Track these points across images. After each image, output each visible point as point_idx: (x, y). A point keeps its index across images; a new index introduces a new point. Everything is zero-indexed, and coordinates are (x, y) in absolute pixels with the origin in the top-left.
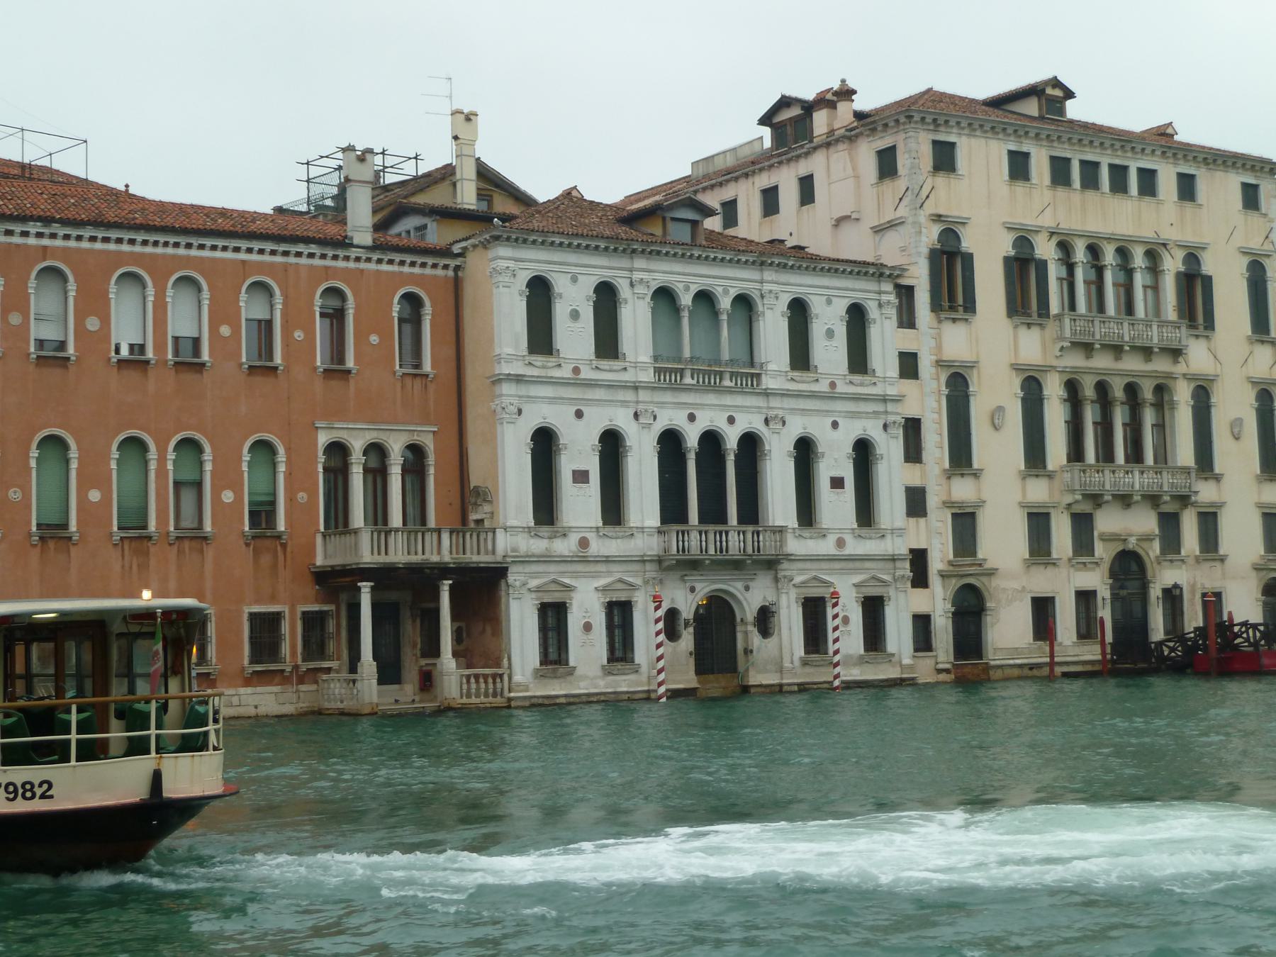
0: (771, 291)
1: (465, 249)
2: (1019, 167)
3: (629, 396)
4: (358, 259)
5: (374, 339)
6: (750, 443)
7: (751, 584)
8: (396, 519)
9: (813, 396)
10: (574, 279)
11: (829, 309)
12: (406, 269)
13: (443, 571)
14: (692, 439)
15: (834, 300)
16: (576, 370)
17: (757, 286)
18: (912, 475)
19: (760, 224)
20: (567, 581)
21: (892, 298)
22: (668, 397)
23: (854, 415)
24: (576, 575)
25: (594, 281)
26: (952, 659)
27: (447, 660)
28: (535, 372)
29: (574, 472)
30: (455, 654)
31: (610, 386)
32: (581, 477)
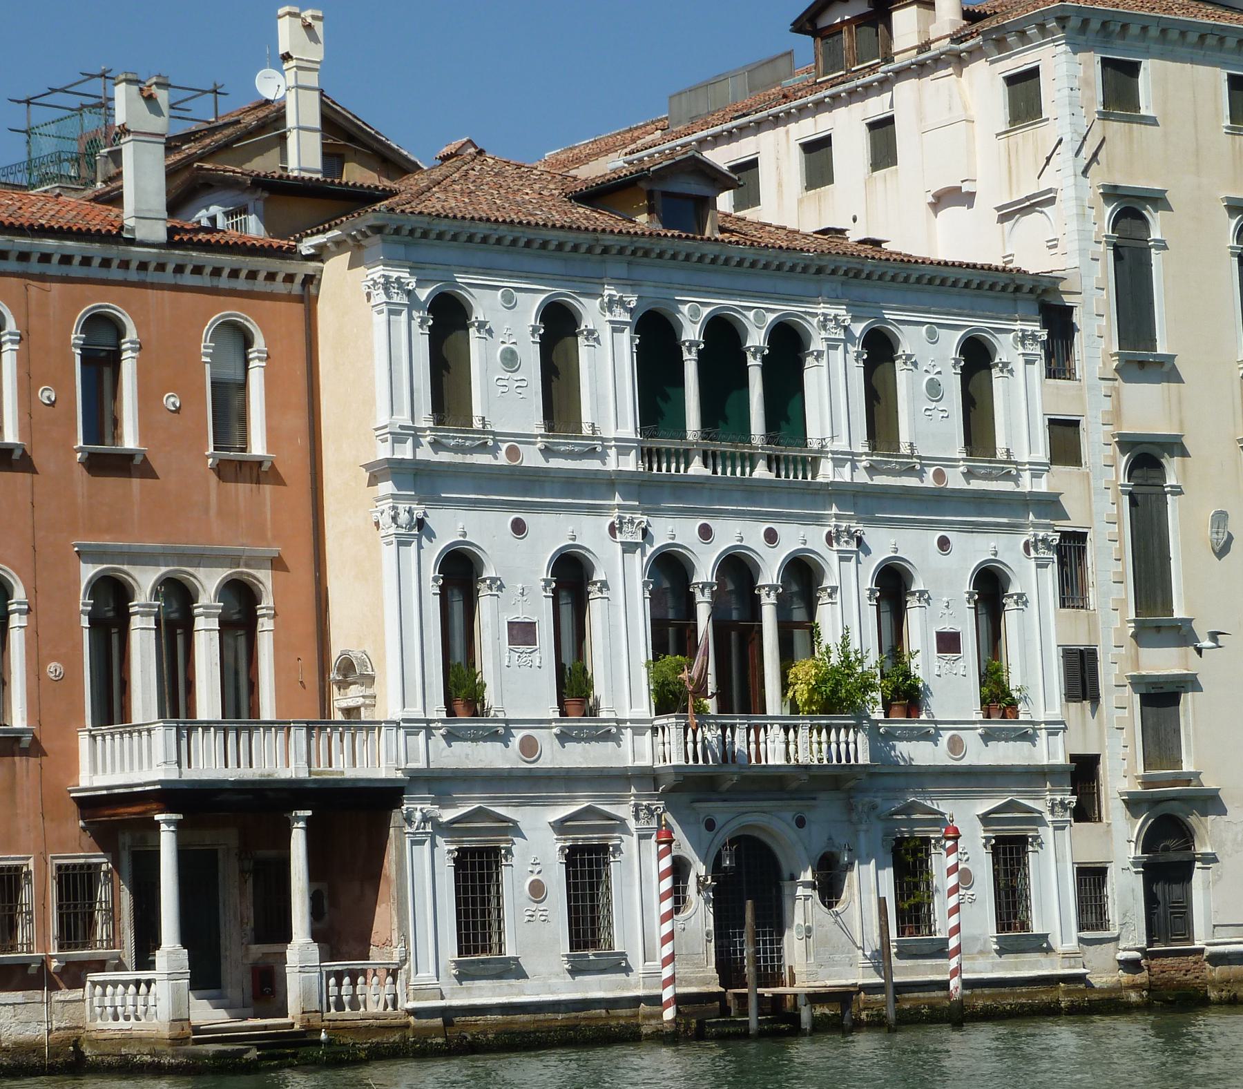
1: (321, 248)
7: (809, 816)
15: (942, 332)
19: (800, 201)
27: (301, 949)
30: (316, 935)
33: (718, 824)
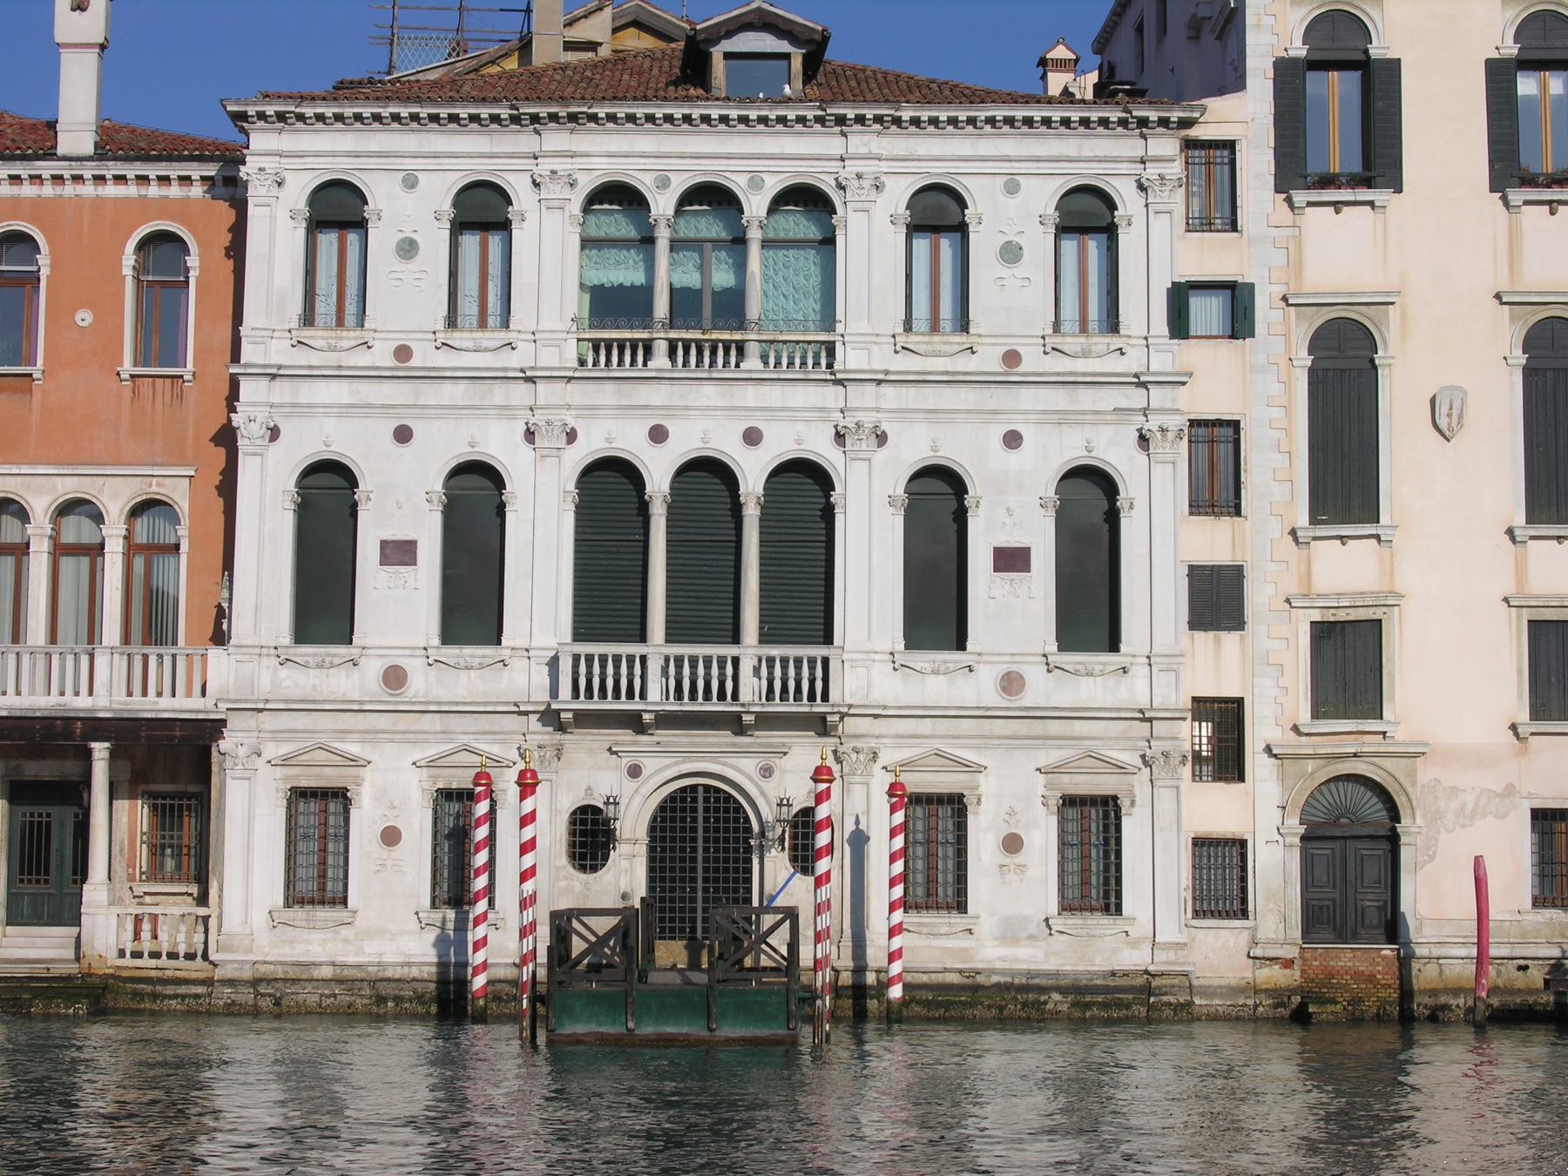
0: (859, 176)
3: (520, 394)
4: (58, 179)
5: (84, 317)
6: (805, 483)
8: (111, 629)
10: (410, 182)
11: (1013, 202)
12: (154, 190)
13: (97, 727)
16: (403, 353)
17: (834, 166)
18: (1213, 541)
20: (353, 748)
21: (1176, 169)
22: (606, 394)
23: (1062, 418)
24: (370, 736)
25: (457, 181)
26: (1297, 934)
28: (315, 359)
29: (384, 544)
31: (476, 378)
32: (399, 553)
33: (645, 773)
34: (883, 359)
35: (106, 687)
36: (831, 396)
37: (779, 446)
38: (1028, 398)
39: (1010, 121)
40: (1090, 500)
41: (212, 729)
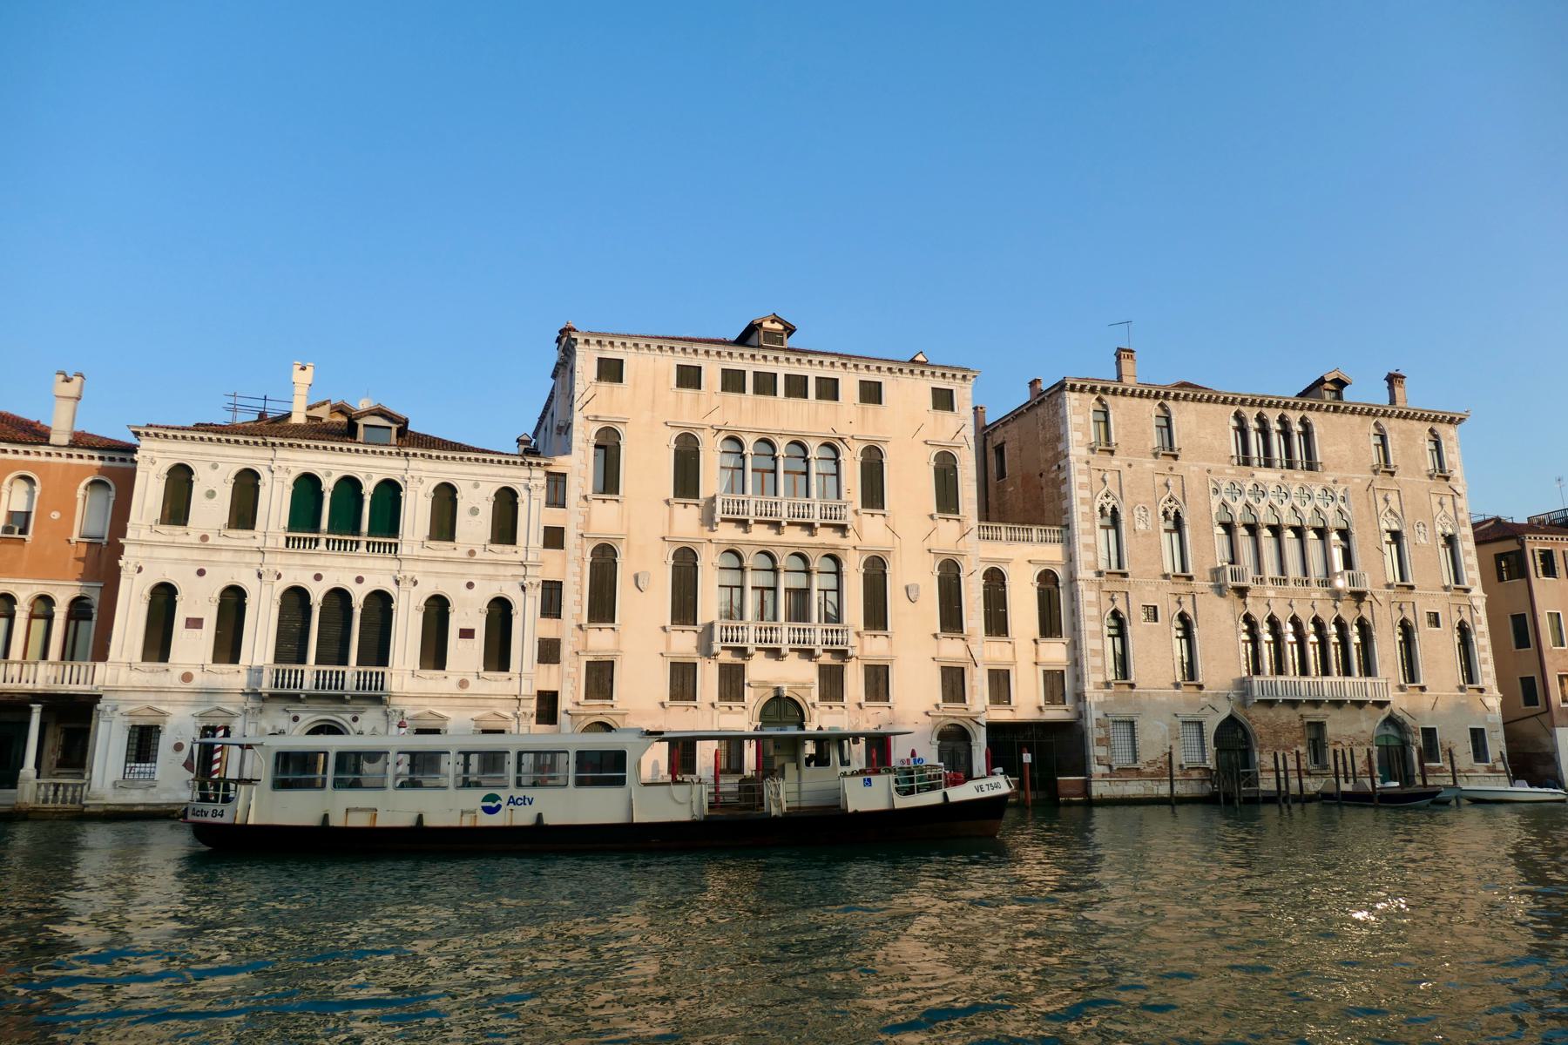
2: (689, 378)
5: (55, 515)
6: (381, 603)
7: (360, 716)
9: (447, 560)
13: (36, 697)
14: (317, 595)
18: (549, 628)
20: (164, 708)
21: (543, 482)
22: (297, 560)
23: (491, 578)
28: (163, 539)
34: (417, 551)
35: (45, 677)
36: (394, 565)
37: (370, 586)
38: (477, 569)
39: (477, 460)
40: (500, 612)
41: (96, 698)
